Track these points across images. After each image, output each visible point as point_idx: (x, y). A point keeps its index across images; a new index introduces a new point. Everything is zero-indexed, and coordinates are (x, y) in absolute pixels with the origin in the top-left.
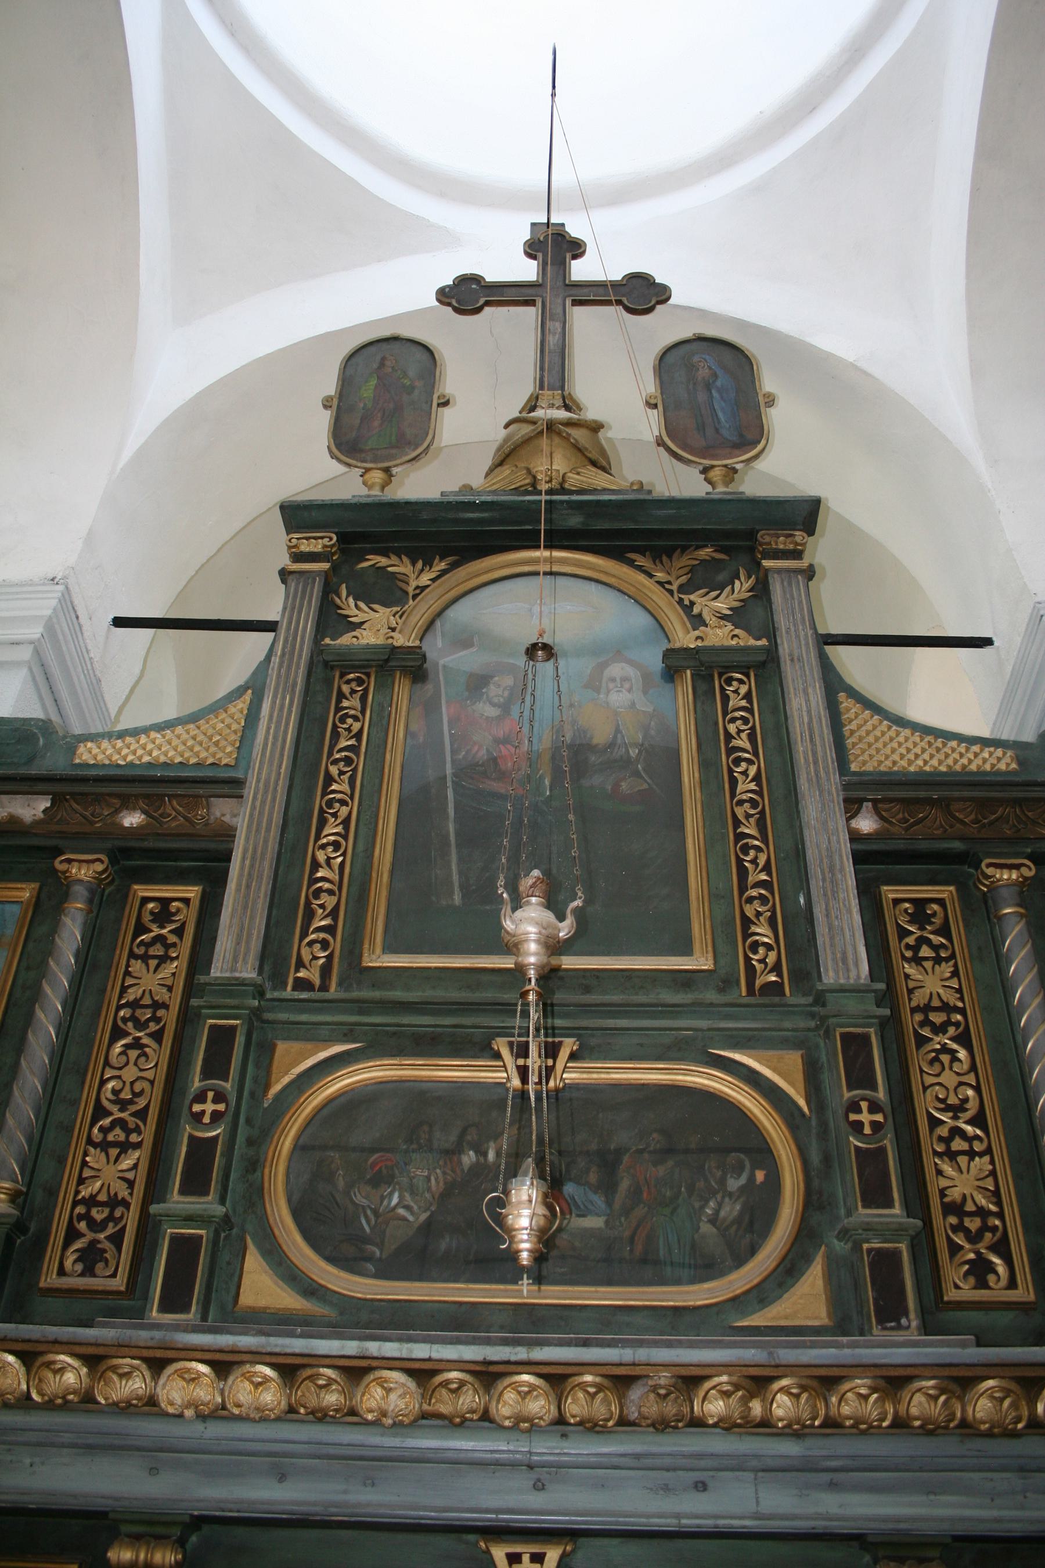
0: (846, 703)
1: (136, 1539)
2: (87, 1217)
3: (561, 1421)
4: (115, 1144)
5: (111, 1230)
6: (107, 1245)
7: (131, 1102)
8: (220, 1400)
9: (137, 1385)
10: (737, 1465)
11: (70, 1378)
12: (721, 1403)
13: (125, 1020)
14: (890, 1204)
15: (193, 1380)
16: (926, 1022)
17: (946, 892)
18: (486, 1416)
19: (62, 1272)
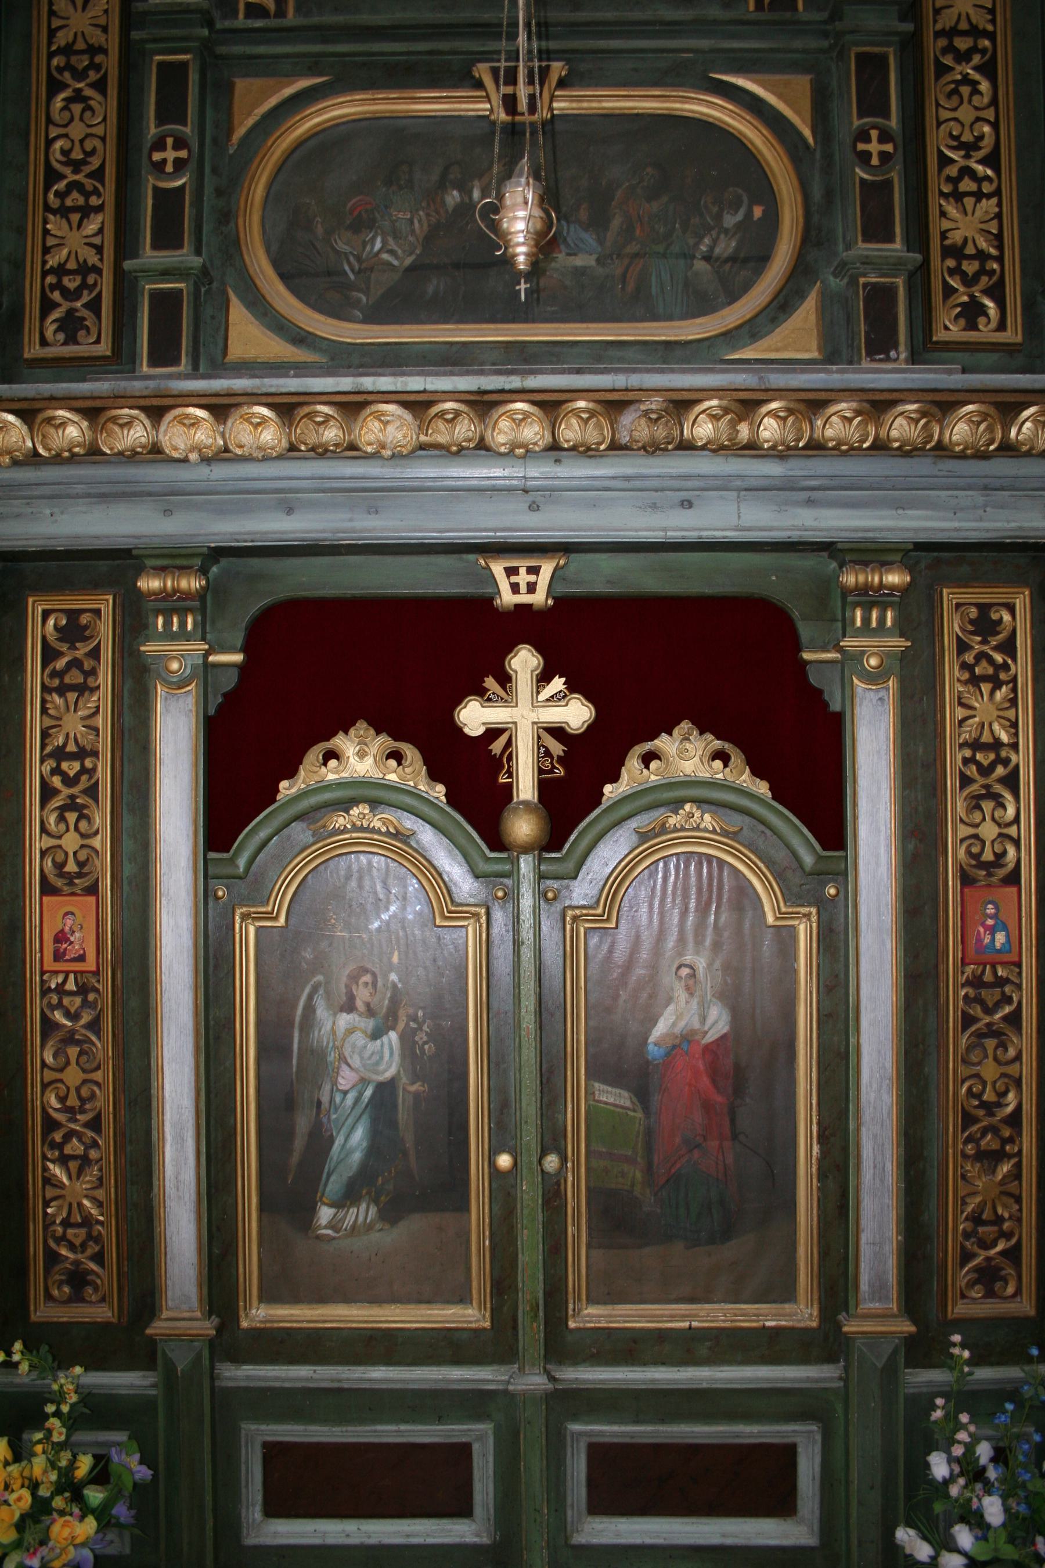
1: (161, 570)
2: (58, 286)
3: (554, 447)
4: (75, 209)
5: (86, 297)
6: (85, 313)
7: (84, 162)
8: (222, 443)
9: (138, 434)
10: (722, 485)
11: (72, 432)
12: (710, 426)
13: (60, 70)
14: (891, 239)
15: (193, 425)
16: (950, 49)
18: (482, 446)
19: (44, 342)
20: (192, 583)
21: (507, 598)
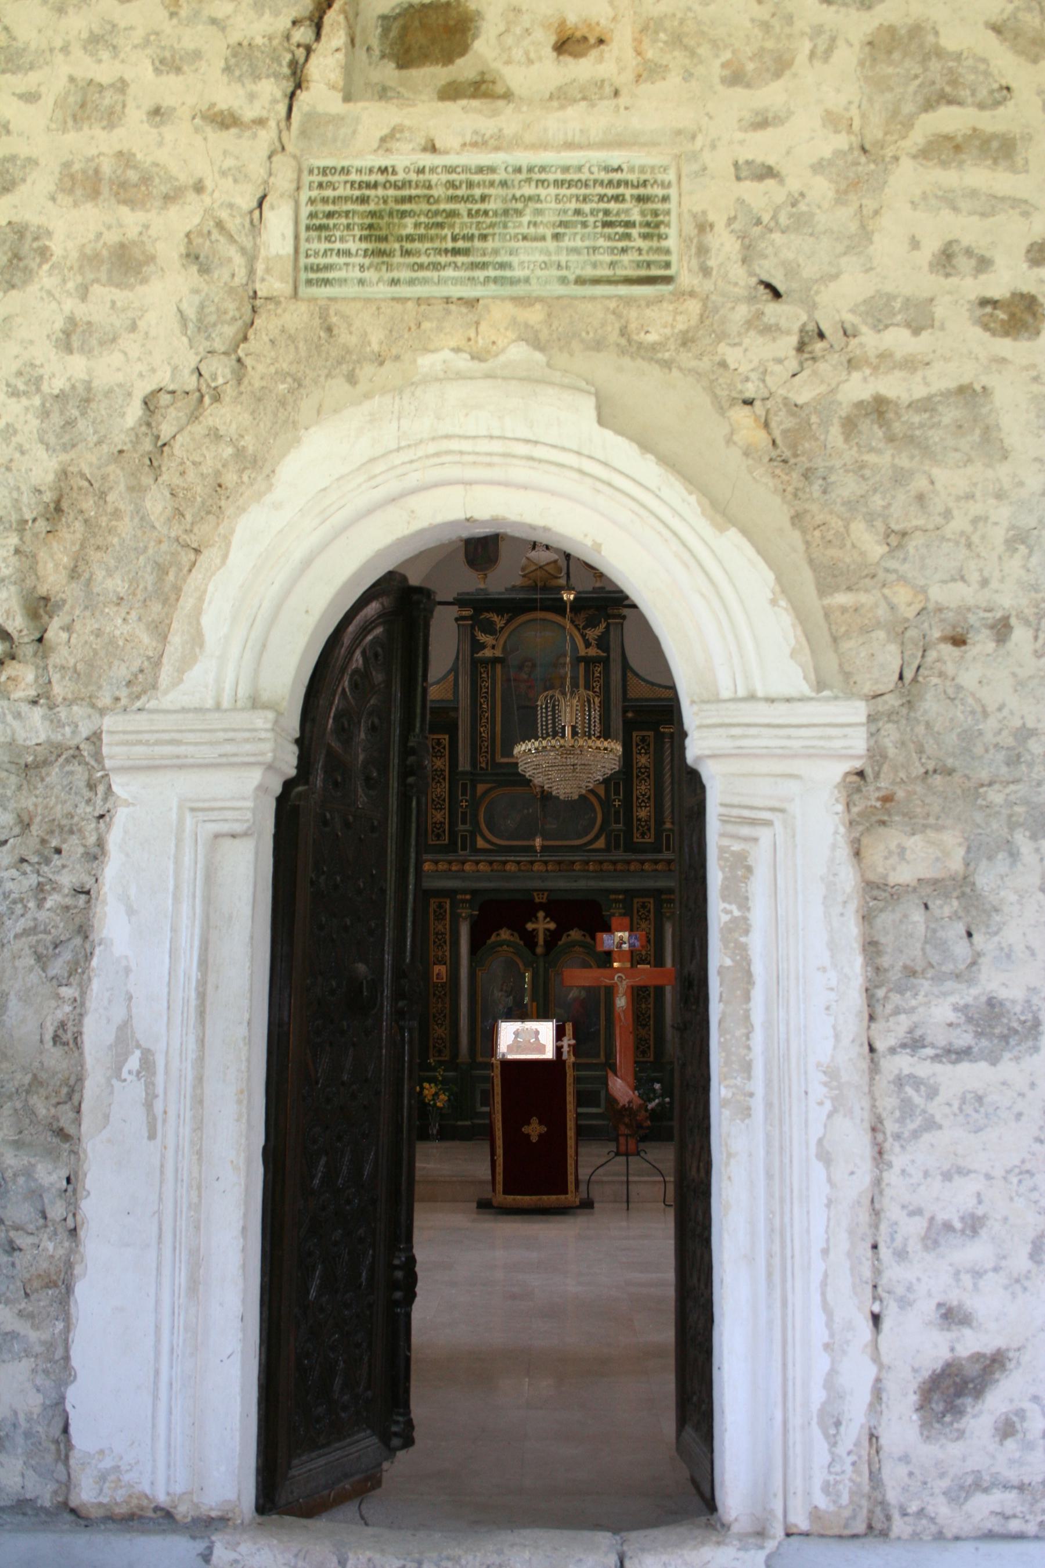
0: (629, 674)
17: (651, 733)
20: (468, 897)
21: (537, 900)
